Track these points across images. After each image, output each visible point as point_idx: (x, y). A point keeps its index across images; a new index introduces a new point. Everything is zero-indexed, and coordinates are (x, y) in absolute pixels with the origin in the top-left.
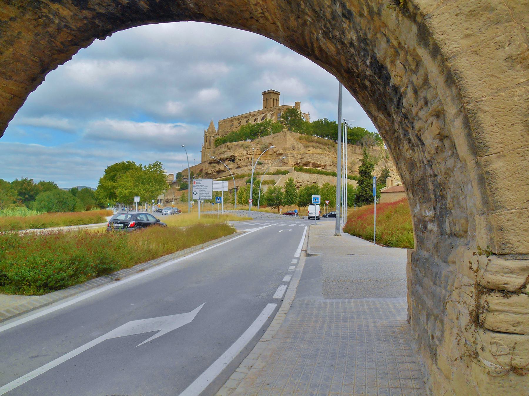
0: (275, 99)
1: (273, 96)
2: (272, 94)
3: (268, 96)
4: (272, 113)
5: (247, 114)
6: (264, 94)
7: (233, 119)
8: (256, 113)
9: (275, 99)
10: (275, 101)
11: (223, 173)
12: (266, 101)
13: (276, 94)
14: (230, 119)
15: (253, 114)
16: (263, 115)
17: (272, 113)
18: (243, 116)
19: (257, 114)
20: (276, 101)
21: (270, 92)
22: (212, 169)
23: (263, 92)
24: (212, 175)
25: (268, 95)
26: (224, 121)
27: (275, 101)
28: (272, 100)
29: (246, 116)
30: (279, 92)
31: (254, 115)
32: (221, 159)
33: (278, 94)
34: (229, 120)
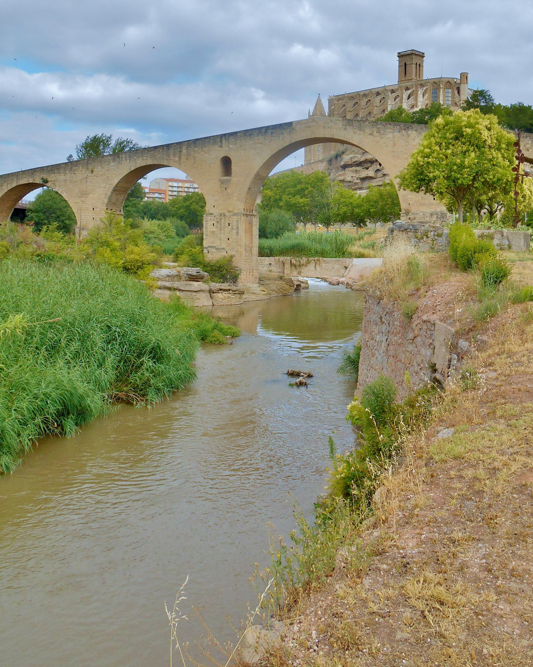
0: (418, 64)
1: (416, 60)
2: (414, 57)
3: (408, 60)
4: (425, 88)
5: (379, 89)
6: (401, 56)
7: (356, 96)
8: (396, 87)
9: (418, 64)
10: (418, 66)
11: (372, 181)
12: (404, 68)
13: (419, 56)
14: (350, 95)
15: (391, 88)
16: (409, 92)
17: (425, 88)
18: (373, 92)
19: (397, 89)
20: (419, 66)
21: (412, 54)
22: (353, 175)
23: (399, 53)
24: (352, 183)
25: (408, 57)
26: (340, 98)
27: (418, 66)
28: (414, 66)
29: (378, 92)
30: (423, 54)
31: (393, 90)
32: (367, 160)
33: (422, 56)
34: (348, 97)
